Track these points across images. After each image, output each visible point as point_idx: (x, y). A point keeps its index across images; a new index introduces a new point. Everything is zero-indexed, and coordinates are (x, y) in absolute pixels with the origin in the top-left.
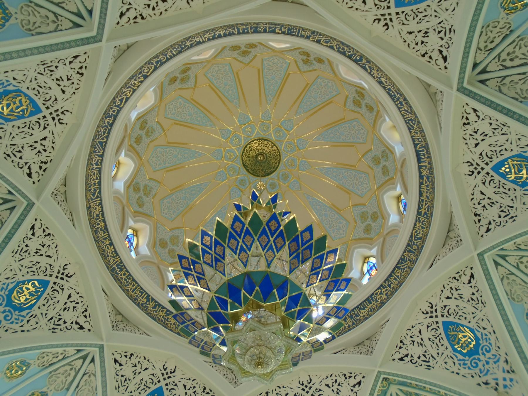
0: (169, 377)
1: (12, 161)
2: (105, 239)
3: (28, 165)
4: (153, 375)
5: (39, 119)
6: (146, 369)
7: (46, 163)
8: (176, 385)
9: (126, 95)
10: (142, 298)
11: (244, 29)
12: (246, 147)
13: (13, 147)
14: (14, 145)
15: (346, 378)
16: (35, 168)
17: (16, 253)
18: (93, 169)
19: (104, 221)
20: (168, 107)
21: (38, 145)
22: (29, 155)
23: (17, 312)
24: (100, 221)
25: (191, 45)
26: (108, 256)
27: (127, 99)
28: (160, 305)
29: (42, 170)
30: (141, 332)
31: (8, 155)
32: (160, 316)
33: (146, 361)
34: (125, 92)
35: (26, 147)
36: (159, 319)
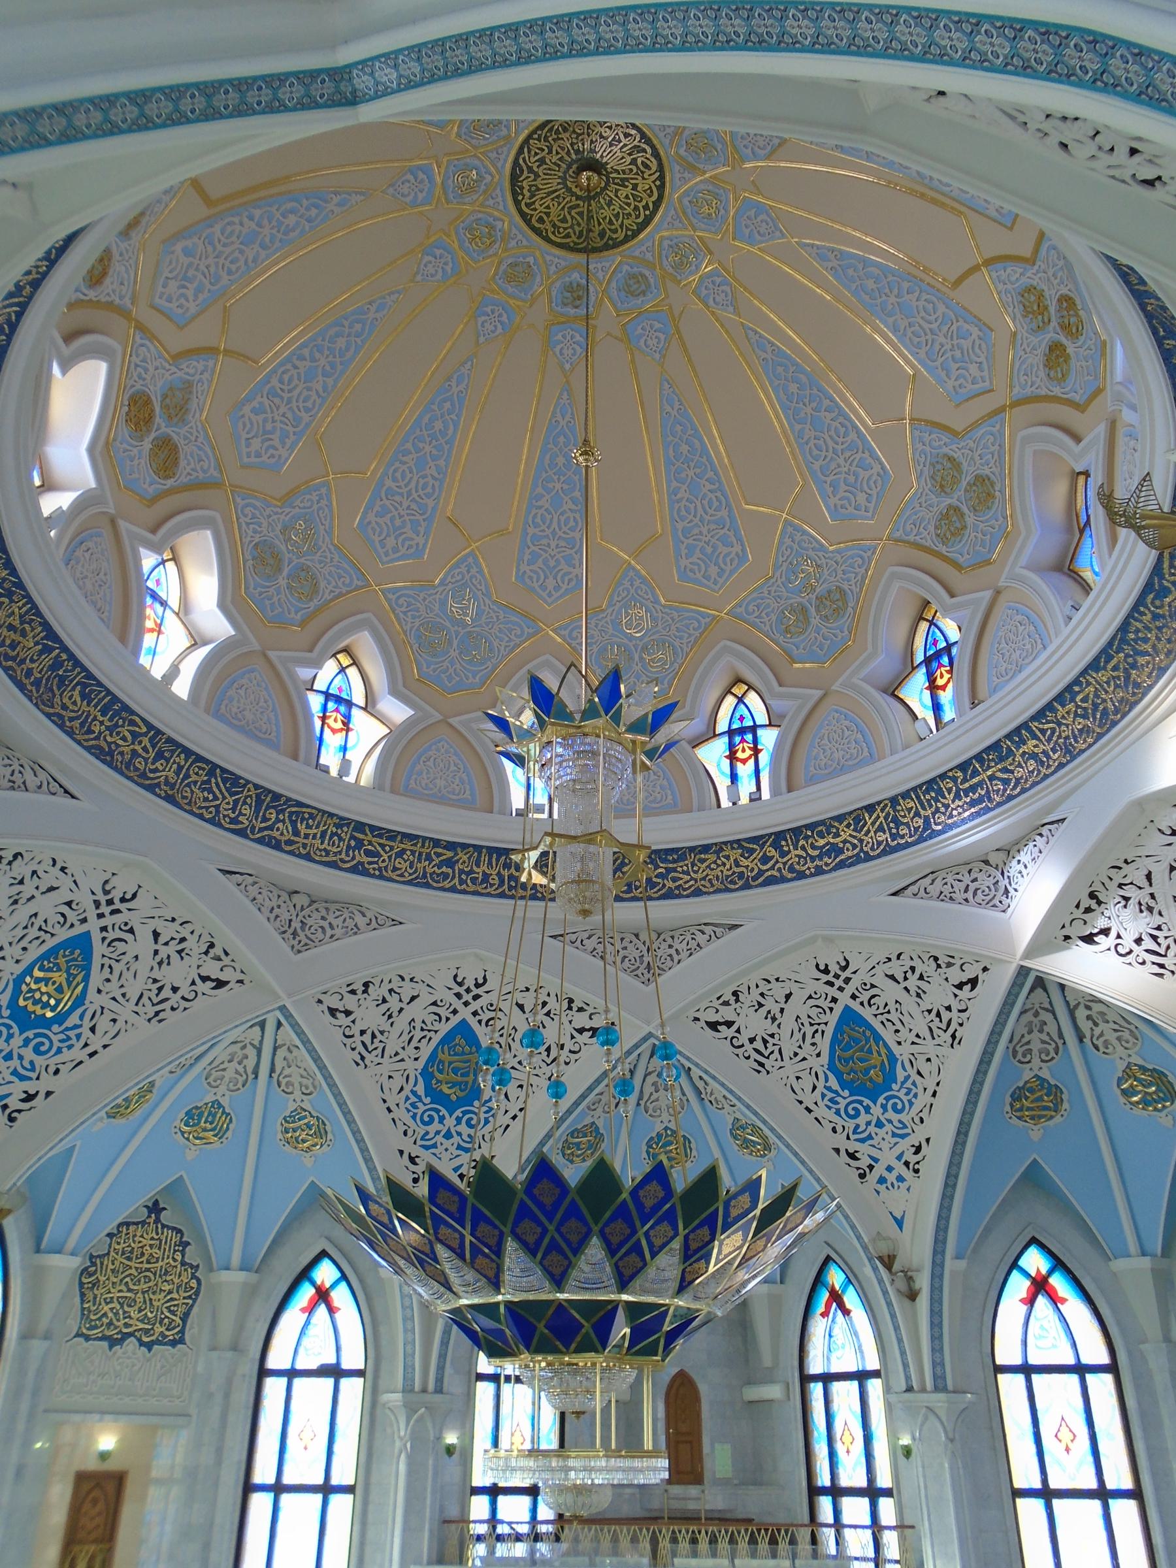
0: (847, 980)
1: (173, 1009)
3: (198, 981)
4: (810, 997)
6: (788, 997)
7: (212, 945)
8: (873, 986)
13: (145, 1000)
14: (141, 995)
16: (212, 969)
17: (363, 1058)
20: (253, 459)
21: (164, 952)
22: (179, 973)
23: (476, 1103)
29: (223, 956)
31: (157, 1014)
33: (774, 984)
35: (156, 974)
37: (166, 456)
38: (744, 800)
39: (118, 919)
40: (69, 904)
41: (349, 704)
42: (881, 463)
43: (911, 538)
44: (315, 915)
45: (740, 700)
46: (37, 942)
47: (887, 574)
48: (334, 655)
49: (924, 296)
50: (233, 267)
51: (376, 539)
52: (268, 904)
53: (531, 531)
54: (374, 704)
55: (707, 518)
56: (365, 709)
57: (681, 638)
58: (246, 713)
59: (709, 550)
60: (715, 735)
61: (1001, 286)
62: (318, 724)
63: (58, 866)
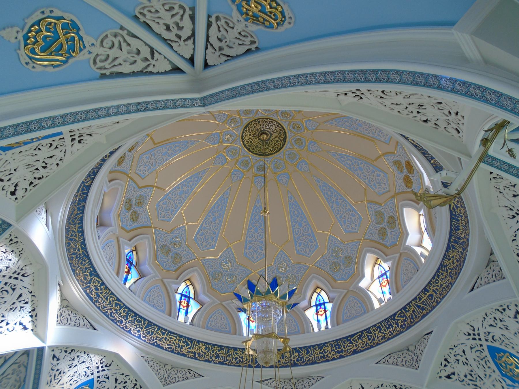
2: (228, 352)
5: (98, 381)
7: (136, 385)
9: (113, 301)
10: (293, 354)
11: (79, 209)
12: (245, 146)
15: (502, 313)
18: (165, 339)
19: (214, 345)
20: (162, 218)
24: (212, 349)
25: (82, 248)
26: (242, 357)
27: (118, 299)
28: (309, 347)
30: (315, 378)
32: (317, 354)
34: (110, 302)
36: (318, 357)
37: (135, 217)
38: (323, 329)
39: (104, 373)
40: (88, 368)
41: (189, 297)
42: (358, 214)
43: (371, 238)
44: (173, 373)
45: (319, 294)
46: (75, 382)
47: (364, 250)
48: (185, 281)
49: (366, 165)
50: (160, 162)
51: (200, 243)
52: (156, 368)
53: (248, 239)
54: (198, 297)
55: (305, 234)
56: (194, 299)
57: (298, 274)
58: (155, 300)
59: (306, 244)
60: (311, 307)
61: (388, 161)
62: (178, 304)
63: (86, 354)
